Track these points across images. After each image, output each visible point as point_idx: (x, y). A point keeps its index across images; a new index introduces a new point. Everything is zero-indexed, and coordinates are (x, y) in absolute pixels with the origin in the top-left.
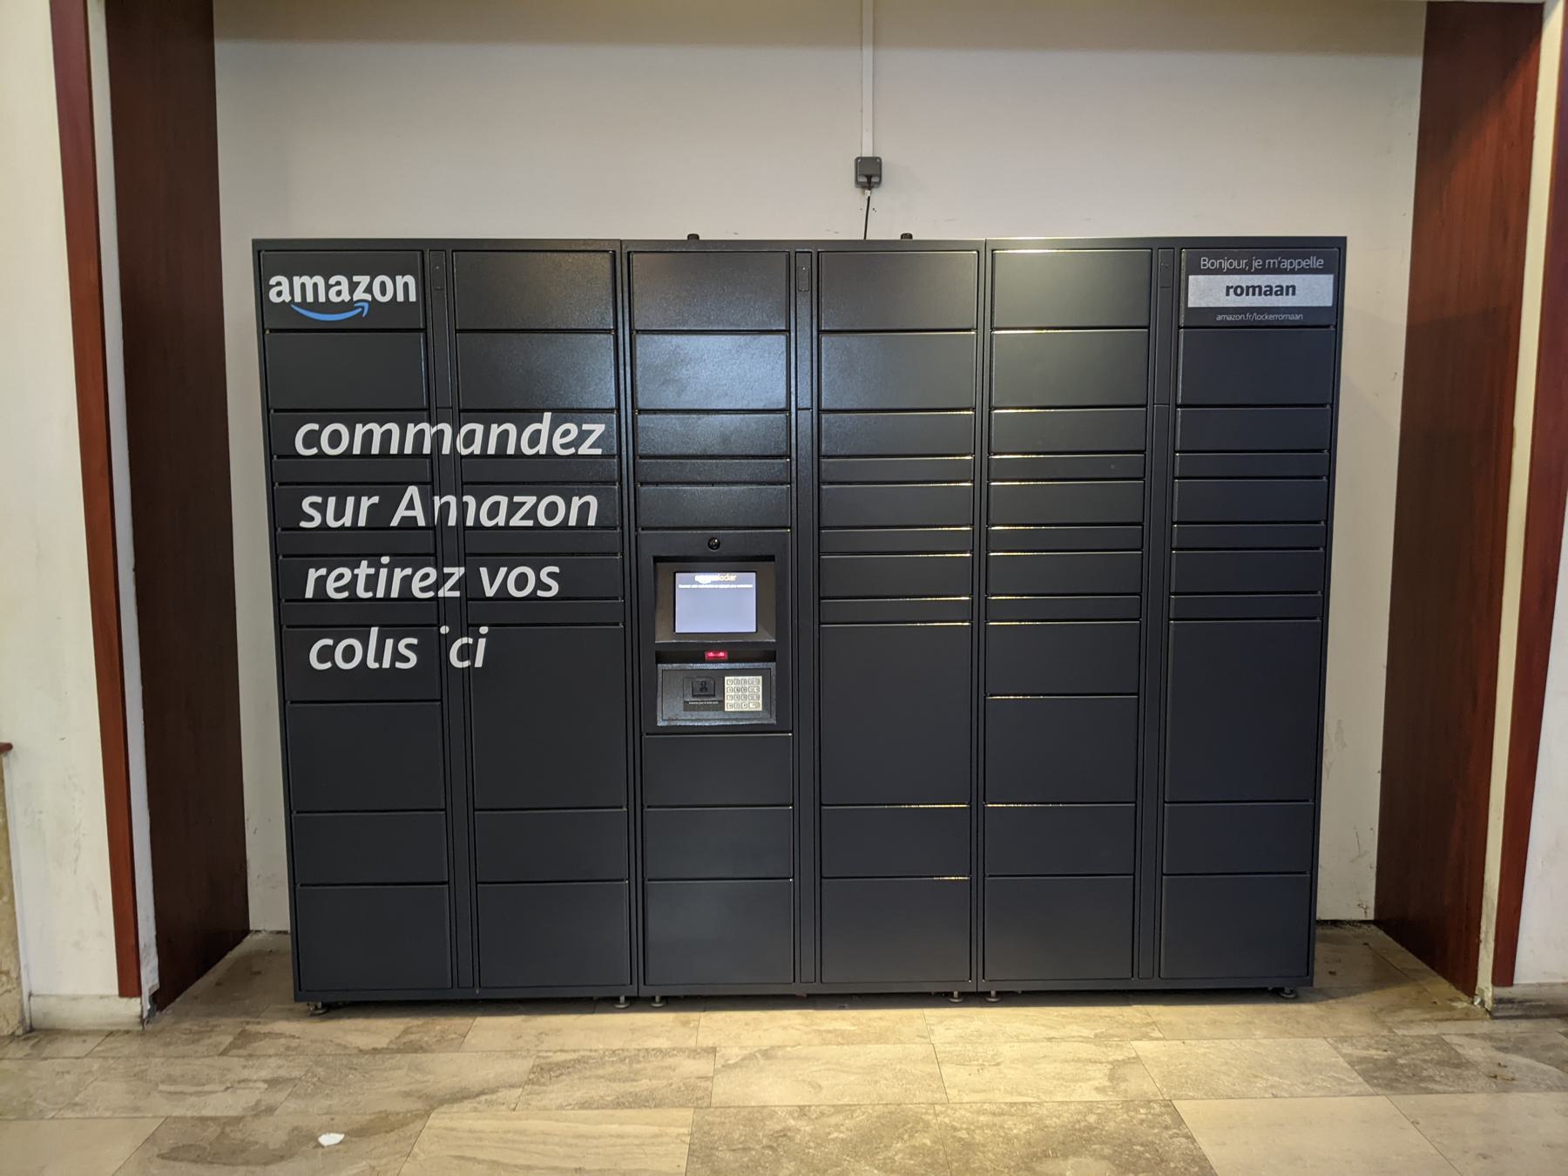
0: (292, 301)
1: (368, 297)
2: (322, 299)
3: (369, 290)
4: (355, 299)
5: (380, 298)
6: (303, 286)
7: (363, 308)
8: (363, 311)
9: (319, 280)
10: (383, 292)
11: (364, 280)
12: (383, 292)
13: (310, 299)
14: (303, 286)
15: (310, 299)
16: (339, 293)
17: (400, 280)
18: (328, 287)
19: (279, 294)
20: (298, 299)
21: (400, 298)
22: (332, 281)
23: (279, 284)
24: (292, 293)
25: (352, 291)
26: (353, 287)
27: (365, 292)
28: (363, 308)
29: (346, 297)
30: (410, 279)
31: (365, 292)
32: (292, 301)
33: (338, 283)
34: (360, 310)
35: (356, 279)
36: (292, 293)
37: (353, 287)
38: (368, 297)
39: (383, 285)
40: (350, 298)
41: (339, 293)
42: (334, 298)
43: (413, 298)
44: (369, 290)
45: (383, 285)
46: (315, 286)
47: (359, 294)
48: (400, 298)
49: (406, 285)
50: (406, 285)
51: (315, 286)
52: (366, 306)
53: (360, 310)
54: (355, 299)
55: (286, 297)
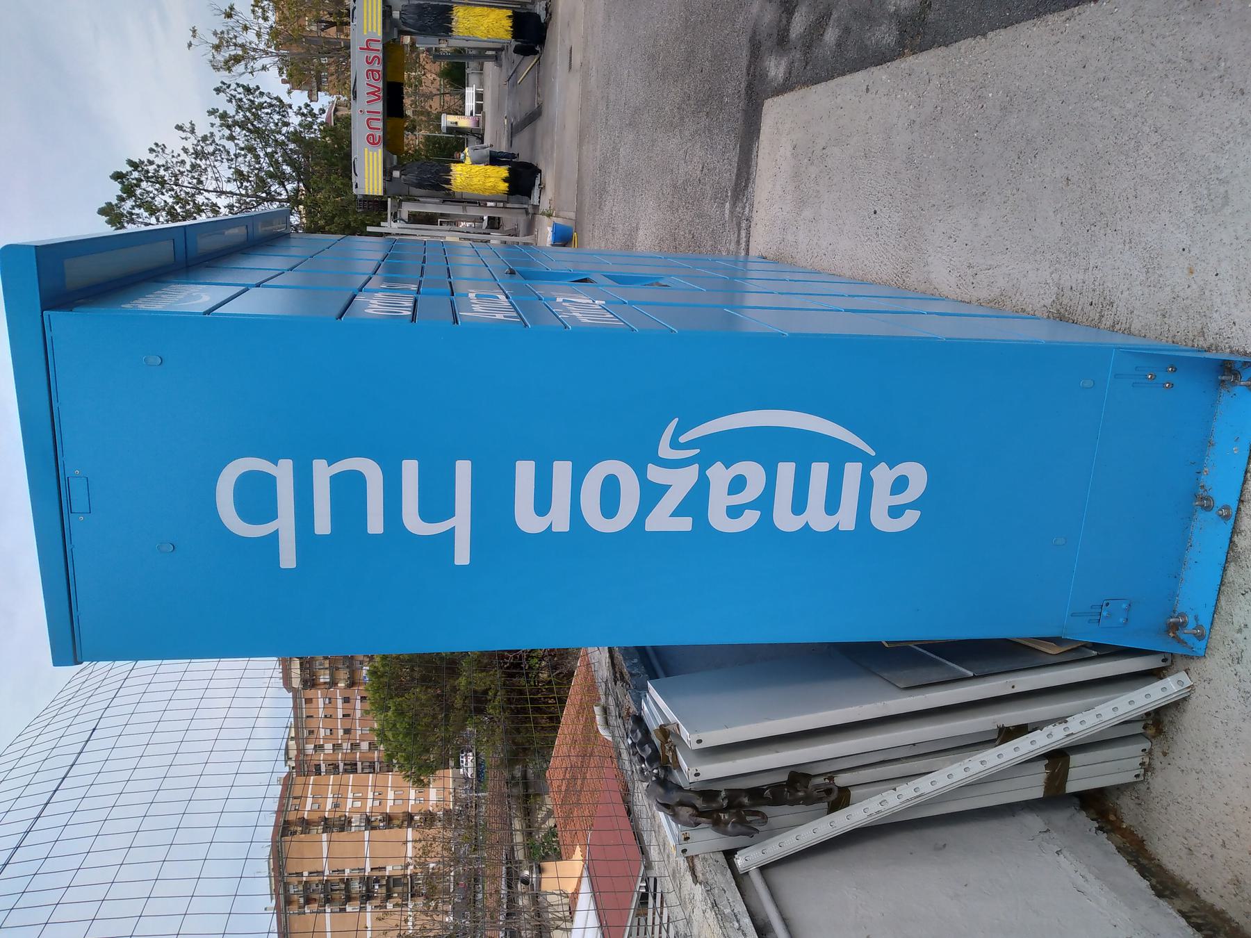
0: (869, 464)
1: (655, 474)
2: (786, 471)
3: (651, 494)
4: (696, 466)
5: (623, 471)
6: (832, 505)
7: (675, 445)
8: (679, 431)
9: (786, 521)
10: (611, 488)
11: (662, 520)
12: (611, 488)
13: (820, 471)
14: (832, 505)
15: (820, 471)
16: (738, 485)
17: (559, 519)
18: (765, 503)
19: (900, 485)
20: (853, 471)
21: (562, 471)
22: (751, 518)
23: (895, 512)
24: (867, 486)
25: (700, 491)
26: (695, 502)
27: (663, 489)
28: (675, 445)
29: (719, 475)
30: (527, 520)
31: (663, 489)
32: (869, 464)
33: (734, 512)
34: (683, 439)
35: (685, 524)
36: (867, 486)
37: (695, 502)
38: (655, 474)
39: (610, 505)
40: (708, 472)
41: (738, 485)
42: (754, 472)
43: (525, 471)
44: (651, 494)
45: (610, 505)
46: (799, 505)
47: (681, 482)
48: (562, 471)
49: (542, 504)
50: (542, 504)
51: (799, 505)
52: (665, 451)
53: (683, 439)
54: (696, 466)
55: (883, 475)
